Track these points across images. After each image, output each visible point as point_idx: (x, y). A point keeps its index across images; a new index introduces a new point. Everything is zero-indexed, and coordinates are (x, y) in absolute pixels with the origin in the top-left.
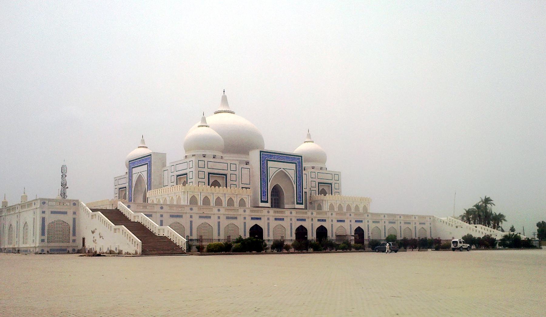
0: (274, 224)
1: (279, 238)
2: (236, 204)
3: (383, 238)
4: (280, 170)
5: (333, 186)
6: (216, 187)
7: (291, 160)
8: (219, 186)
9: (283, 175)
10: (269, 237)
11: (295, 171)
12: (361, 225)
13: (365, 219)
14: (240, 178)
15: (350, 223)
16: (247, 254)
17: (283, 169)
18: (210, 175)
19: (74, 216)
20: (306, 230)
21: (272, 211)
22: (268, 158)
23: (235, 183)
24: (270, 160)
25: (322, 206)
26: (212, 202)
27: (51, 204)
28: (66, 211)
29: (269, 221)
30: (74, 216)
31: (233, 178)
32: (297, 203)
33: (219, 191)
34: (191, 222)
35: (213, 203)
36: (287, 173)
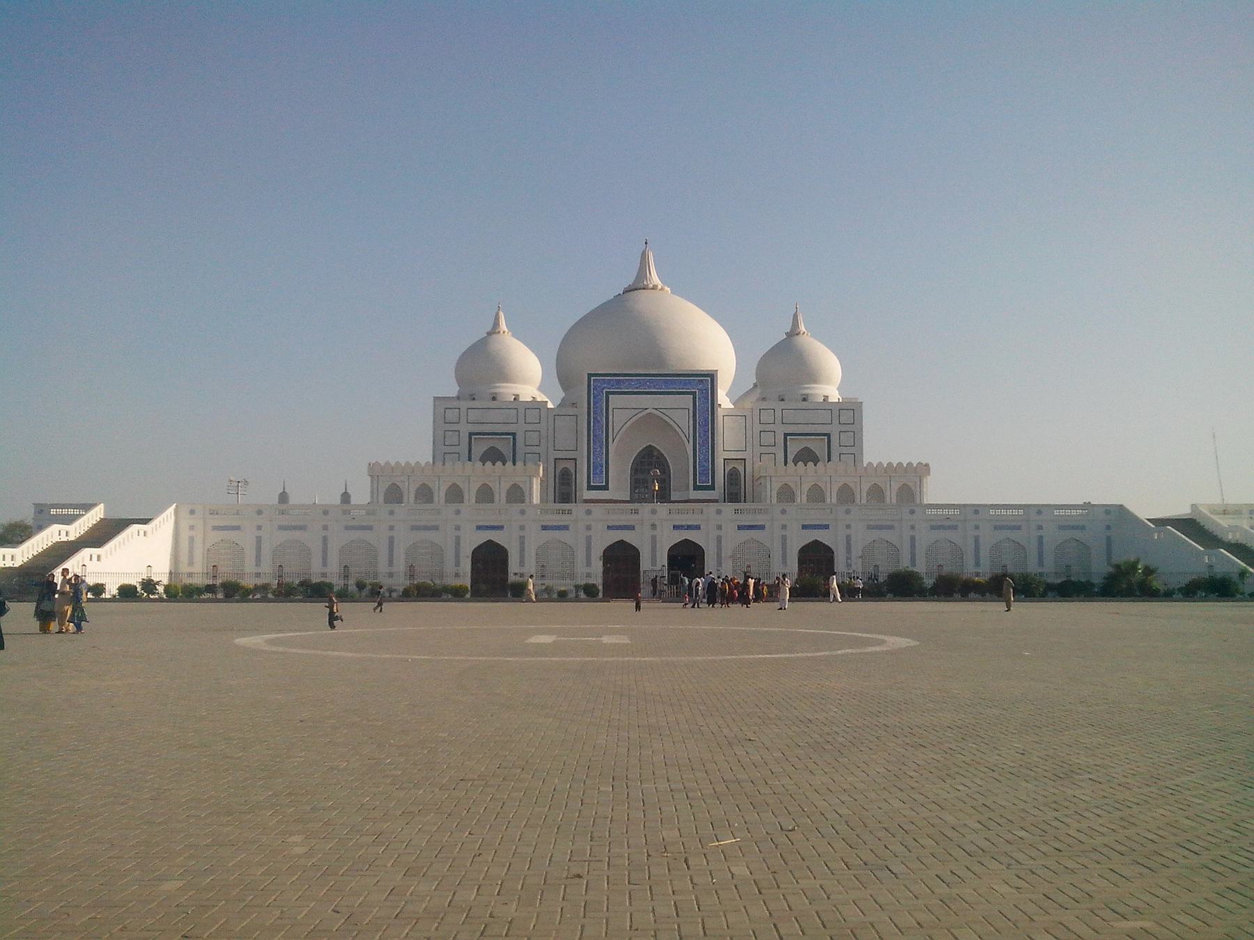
0: (733, 539)
1: (871, 569)
2: (831, 498)
3: (297, 582)
4: (648, 411)
5: (834, 439)
6: (810, 462)
7: (682, 387)
8: (816, 460)
9: (652, 421)
10: (718, 566)
11: (691, 414)
12: (823, 537)
13: (965, 520)
14: (551, 438)
15: (718, 533)
16: (956, 601)
17: (656, 409)
18: (473, 437)
19: (457, 533)
20: (829, 551)
21: (728, 508)
22: (609, 388)
23: (536, 449)
24: (694, 398)
25: (527, 494)
26: (829, 494)
27: (55, 513)
28: (565, 523)
29: (589, 533)
30: (457, 533)
31: (533, 438)
32: (696, 488)
33: (807, 475)
34: (325, 539)
35: (440, 494)
36: (666, 418)
